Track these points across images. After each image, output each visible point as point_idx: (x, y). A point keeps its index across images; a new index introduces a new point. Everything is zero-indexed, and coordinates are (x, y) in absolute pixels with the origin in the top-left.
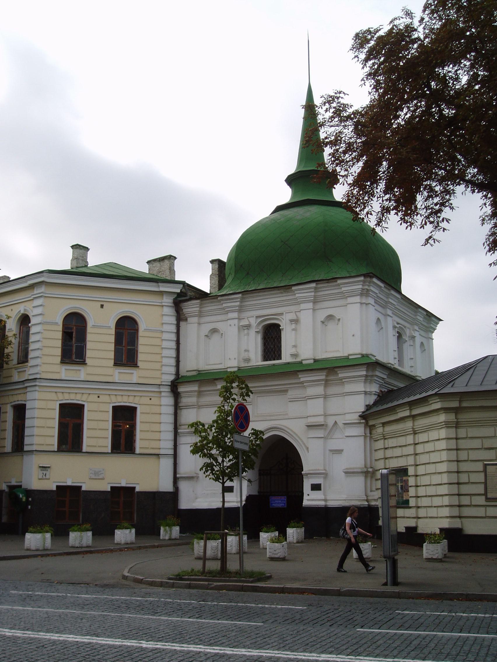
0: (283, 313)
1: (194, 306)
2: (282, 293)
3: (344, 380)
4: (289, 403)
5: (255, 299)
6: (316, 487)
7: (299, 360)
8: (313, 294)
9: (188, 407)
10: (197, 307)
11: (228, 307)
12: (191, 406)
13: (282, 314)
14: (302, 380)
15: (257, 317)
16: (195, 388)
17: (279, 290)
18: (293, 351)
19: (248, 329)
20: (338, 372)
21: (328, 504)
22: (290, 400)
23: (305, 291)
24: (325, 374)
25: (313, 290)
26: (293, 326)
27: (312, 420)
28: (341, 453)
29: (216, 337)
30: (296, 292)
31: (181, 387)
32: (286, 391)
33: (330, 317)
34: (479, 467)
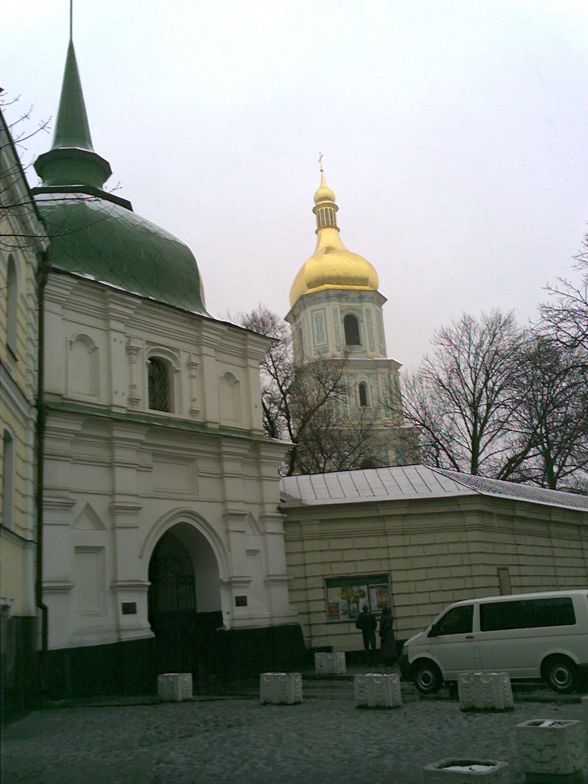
0: (179, 350)
1: (64, 286)
2: (185, 322)
3: (262, 460)
4: (200, 479)
5: (163, 318)
6: (241, 602)
7: (199, 419)
8: (218, 338)
9: (57, 457)
10: (67, 290)
11: (116, 311)
12: (63, 456)
13: (177, 350)
14: (224, 449)
15: (148, 342)
16: (75, 426)
17: (184, 316)
18: (197, 406)
19: (136, 354)
20: (262, 449)
21: (274, 623)
22: (200, 474)
23: (214, 332)
24: (248, 447)
25: (221, 334)
26: (194, 373)
27: (232, 507)
28: (254, 555)
29: (80, 350)
30: (205, 329)
31: (53, 418)
32: (191, 460)
33: (229, 376)
34: (493, 571)
